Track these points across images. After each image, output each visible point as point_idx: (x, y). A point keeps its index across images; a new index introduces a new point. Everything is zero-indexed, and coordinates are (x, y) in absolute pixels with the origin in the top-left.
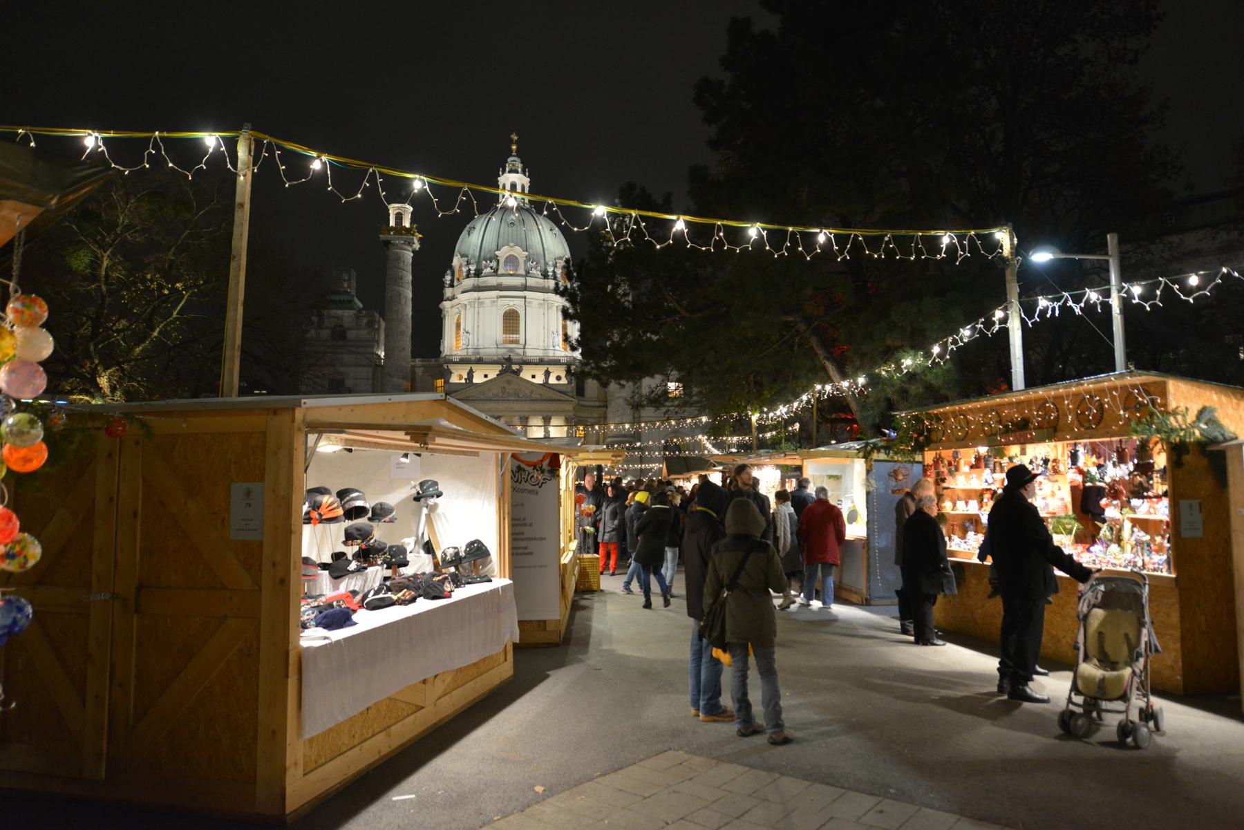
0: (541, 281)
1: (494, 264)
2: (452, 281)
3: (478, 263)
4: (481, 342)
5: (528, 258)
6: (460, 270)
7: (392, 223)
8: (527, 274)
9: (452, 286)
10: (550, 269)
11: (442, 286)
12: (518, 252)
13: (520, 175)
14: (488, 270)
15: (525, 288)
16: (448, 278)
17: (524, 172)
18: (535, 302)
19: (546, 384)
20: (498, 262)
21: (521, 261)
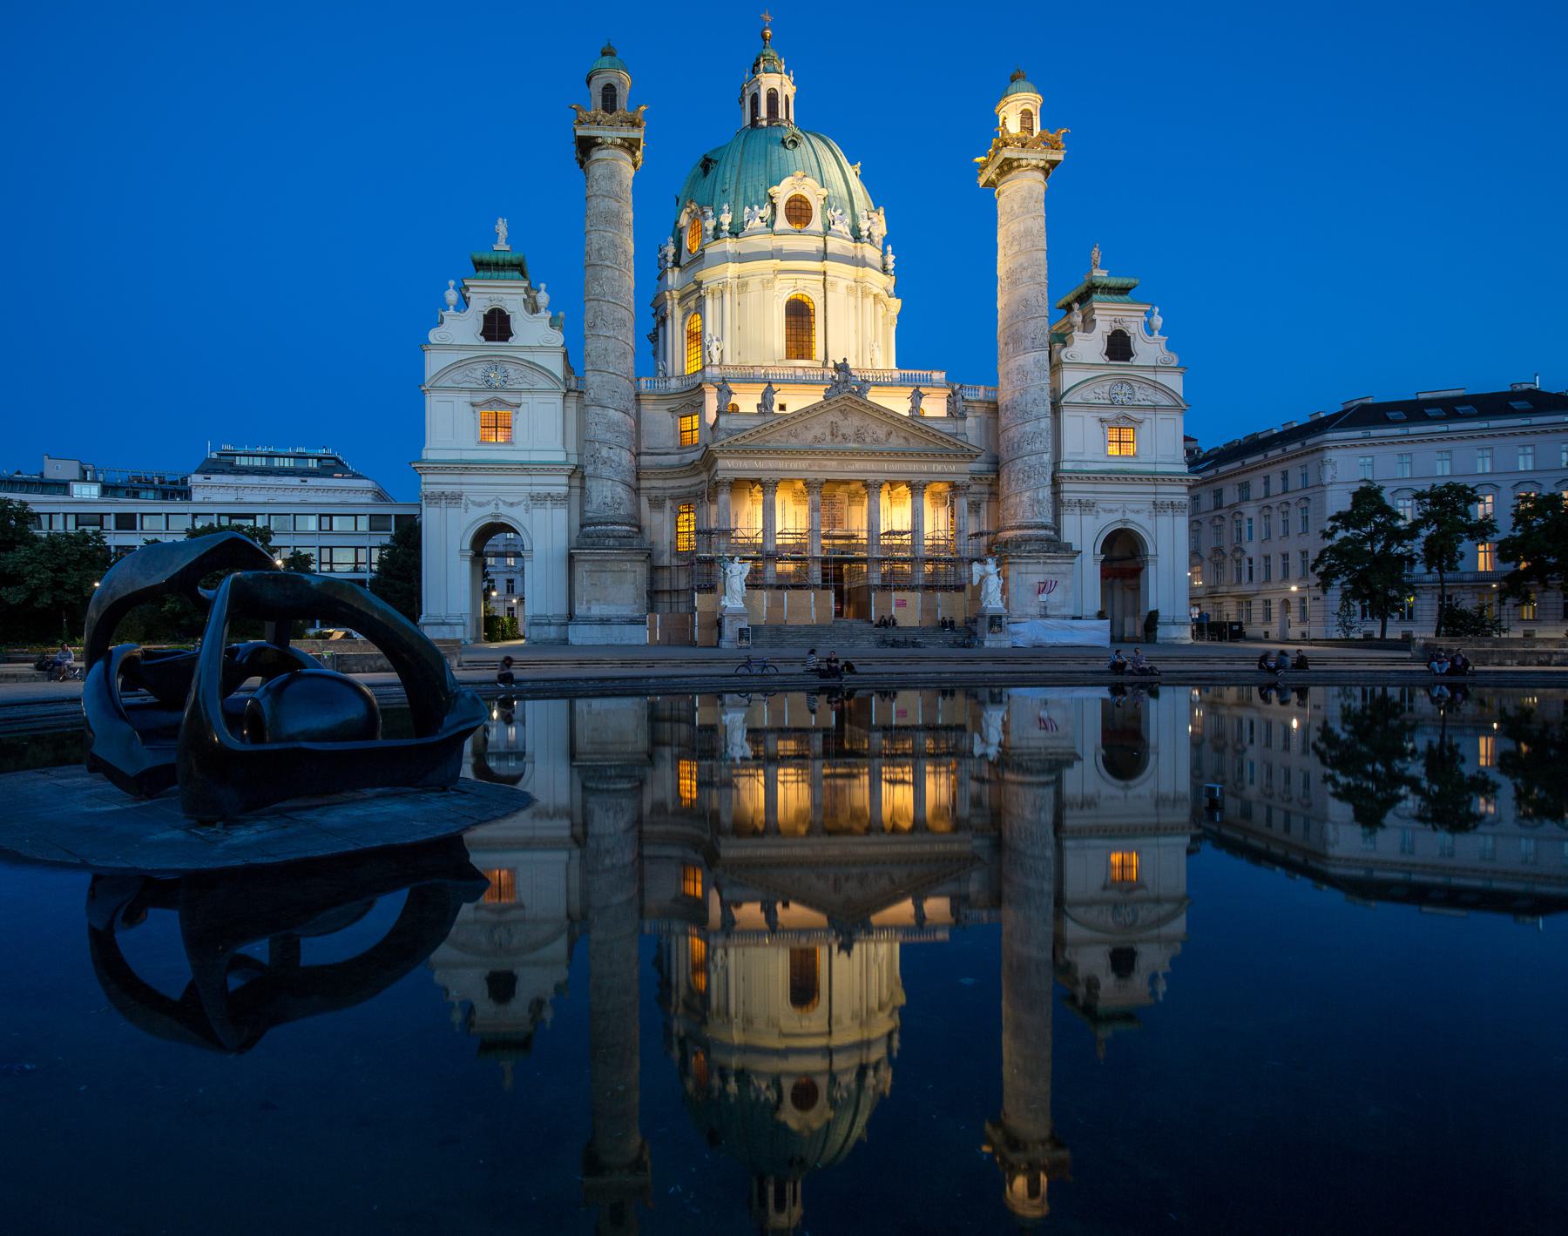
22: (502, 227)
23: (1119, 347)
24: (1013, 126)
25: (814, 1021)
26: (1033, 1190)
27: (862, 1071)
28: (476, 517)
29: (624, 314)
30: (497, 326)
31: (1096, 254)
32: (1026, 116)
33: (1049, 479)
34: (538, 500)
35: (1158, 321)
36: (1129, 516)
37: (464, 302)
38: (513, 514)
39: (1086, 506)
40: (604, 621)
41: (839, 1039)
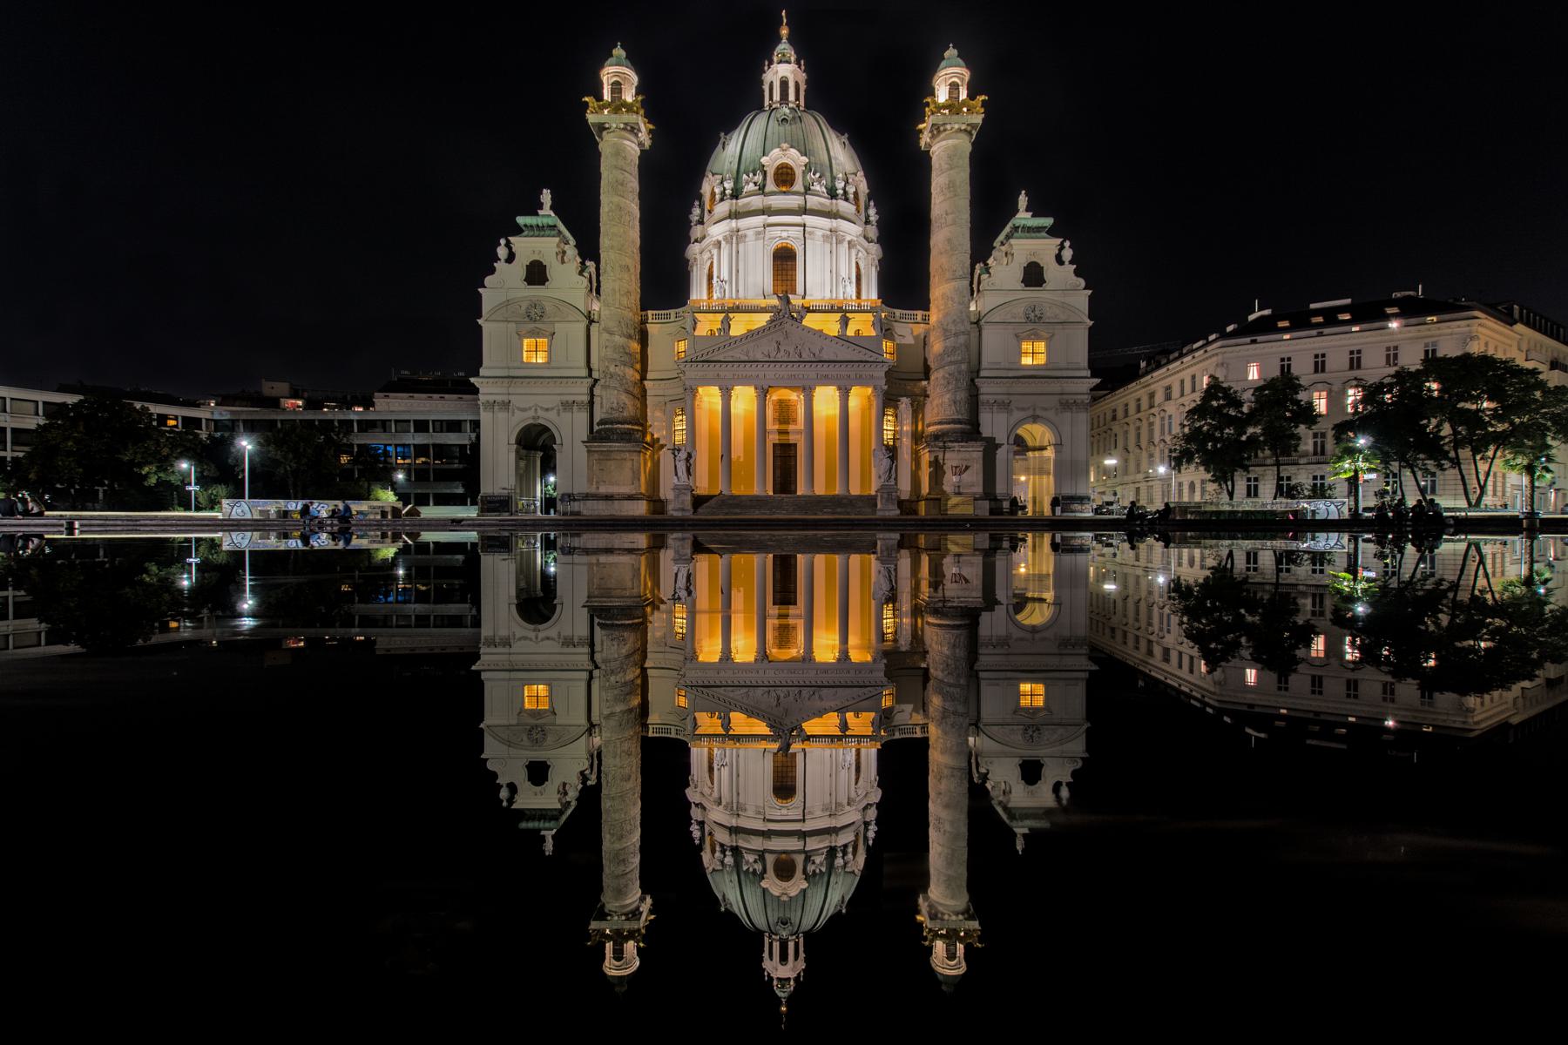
0: (827, 202)
1: (759, 178)
2: (702, 216)
3: (737, 180)
4: (741, 294)
5: (808, 168)
6: (713, 194)
7: (607, 96)
8: (807, 190)
9: (701, 222)
10: (840, 185)
11: (687, 226)
12: (795, 159)
13: (793, 66)
14: (751, 187)
15: (804, 211)
16: (696, 211)
17: (798, 62)
18: (819, 233)
19: (842, 338)
20: (765, 174)
21: (798, 172)
22: (546, 197)
23: (1033, 275)
24: (942, 95)
25: (791, 810)
26: (951, 956)
27: (832, 852)
28: (520, 420)
29: (629, 261)
30: (536, 274)
31: (1023, 200)
32: (954, 87)
33: (964, 384)
34: (568, 406)
35: (1068, 254)
36: (1038, 412)
37: (511, 258)
38: (548, 418)
39: (1005, 406)
40: (609, 498)
41: (808, 826)
